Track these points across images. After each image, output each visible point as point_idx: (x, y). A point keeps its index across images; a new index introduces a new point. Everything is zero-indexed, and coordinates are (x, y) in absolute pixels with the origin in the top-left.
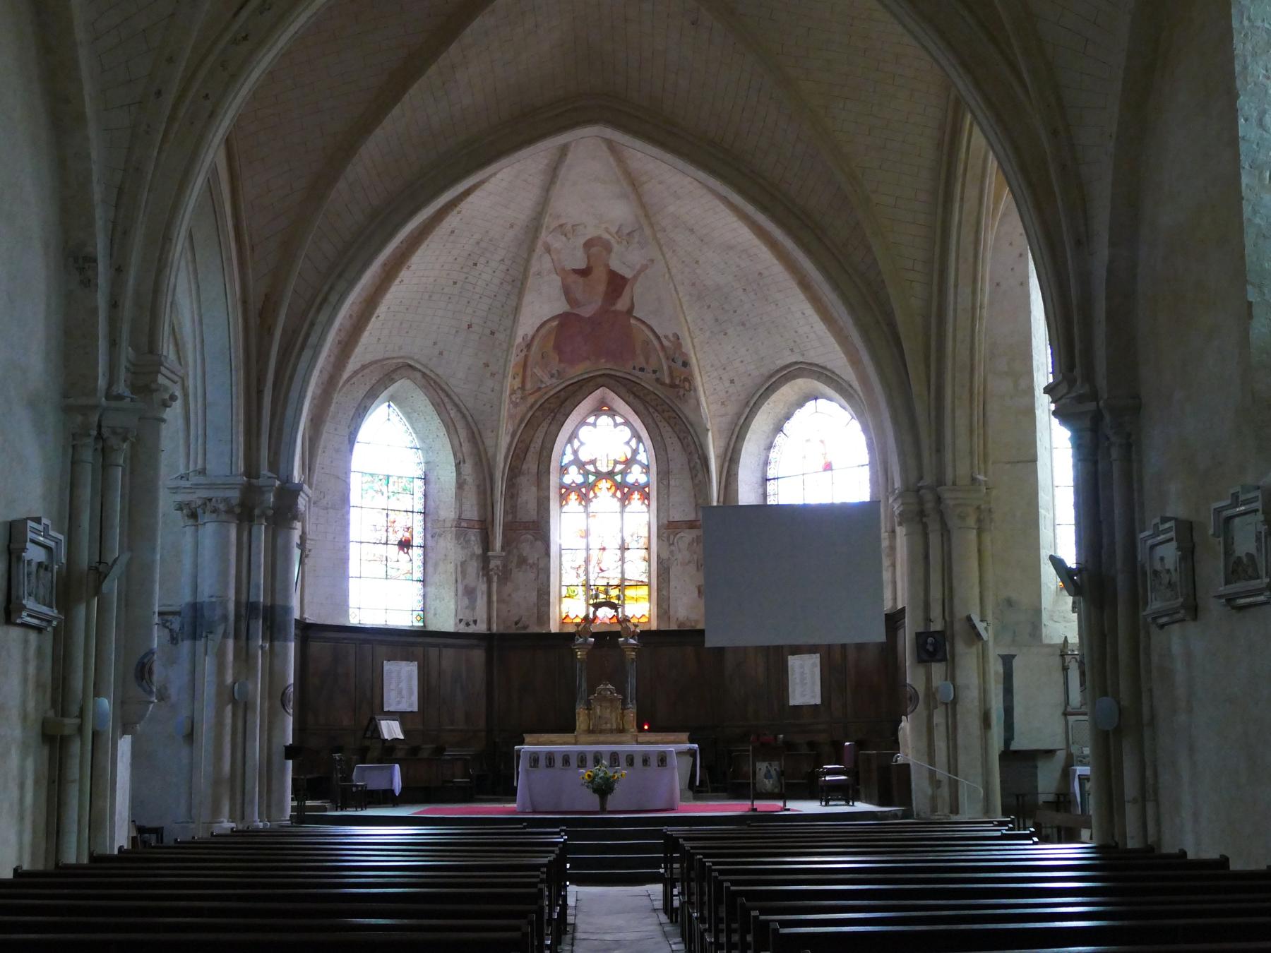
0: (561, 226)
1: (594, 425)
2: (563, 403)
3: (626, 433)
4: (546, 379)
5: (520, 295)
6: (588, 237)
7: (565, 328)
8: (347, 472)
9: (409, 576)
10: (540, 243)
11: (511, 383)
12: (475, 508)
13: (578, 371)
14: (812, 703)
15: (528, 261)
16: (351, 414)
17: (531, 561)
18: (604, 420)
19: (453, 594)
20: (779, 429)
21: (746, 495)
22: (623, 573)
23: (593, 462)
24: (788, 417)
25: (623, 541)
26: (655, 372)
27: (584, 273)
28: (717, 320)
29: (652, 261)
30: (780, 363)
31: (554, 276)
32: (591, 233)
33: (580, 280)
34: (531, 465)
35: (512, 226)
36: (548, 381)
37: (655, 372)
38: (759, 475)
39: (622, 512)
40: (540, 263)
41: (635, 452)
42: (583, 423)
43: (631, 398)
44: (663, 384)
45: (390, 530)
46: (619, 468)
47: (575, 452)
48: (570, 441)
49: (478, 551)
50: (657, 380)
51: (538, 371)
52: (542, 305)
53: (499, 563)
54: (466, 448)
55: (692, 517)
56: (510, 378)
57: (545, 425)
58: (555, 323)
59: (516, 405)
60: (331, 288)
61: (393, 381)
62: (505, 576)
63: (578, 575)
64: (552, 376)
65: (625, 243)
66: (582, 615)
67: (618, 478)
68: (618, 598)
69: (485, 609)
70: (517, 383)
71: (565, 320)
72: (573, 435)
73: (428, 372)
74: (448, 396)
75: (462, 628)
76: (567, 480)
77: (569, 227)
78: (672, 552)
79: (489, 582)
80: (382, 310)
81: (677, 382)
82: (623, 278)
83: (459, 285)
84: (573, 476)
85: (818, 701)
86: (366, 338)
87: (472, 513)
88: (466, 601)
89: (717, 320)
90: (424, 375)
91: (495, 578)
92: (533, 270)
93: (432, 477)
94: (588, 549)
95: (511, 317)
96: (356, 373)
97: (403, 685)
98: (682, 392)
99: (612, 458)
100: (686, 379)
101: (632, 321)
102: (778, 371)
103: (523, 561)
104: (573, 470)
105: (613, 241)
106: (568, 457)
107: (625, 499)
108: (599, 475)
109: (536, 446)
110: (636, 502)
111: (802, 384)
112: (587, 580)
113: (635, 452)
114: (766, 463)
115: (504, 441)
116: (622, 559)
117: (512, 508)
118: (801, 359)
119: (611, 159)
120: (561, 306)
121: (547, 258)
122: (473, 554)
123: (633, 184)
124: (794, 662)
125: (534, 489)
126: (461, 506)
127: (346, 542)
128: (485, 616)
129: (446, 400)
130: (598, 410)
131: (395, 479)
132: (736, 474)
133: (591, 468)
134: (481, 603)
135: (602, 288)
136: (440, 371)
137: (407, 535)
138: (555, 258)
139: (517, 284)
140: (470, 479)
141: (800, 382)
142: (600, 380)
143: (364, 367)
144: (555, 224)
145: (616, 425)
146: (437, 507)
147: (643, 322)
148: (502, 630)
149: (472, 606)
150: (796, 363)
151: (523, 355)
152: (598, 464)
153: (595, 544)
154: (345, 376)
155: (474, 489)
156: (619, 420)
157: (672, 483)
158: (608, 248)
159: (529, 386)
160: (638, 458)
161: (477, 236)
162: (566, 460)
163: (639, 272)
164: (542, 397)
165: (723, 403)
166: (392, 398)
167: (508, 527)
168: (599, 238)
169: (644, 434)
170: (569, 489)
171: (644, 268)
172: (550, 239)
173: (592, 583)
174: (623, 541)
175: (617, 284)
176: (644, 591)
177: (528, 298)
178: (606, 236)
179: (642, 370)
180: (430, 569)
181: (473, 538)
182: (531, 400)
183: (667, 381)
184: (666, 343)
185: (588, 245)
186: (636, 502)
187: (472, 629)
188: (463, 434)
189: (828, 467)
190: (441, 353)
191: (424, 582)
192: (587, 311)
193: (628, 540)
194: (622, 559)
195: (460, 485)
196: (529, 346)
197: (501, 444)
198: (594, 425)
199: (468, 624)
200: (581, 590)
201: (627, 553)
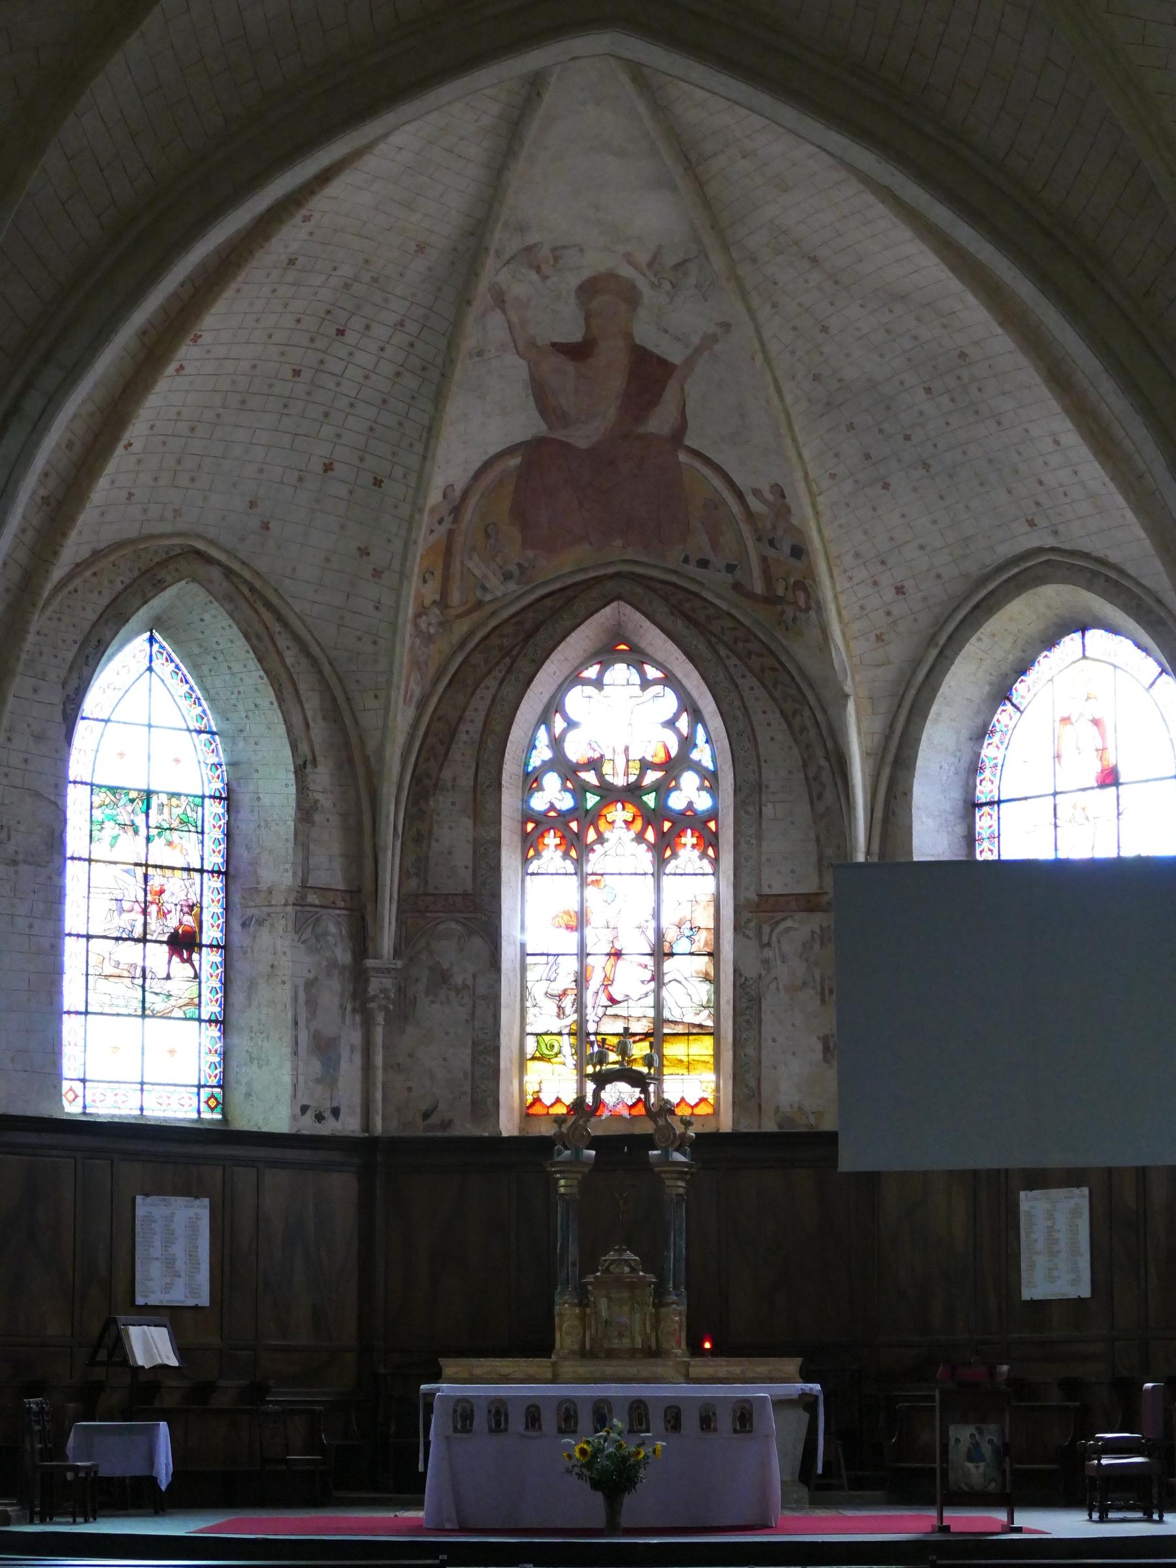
0: (529, 249)
1: (598, 683)
2: (529, 636)
3: (669, 702)
4: (494, 582)
5: (439, 397)
6: (586, 274)
7: (536, 472)
8: (60, 782)
9: (192, 1011)
10: (483, 285)
11: (418, 590)
12: (337, 865)
13: (566, 565)
14: (1071, 1293)
15: (457, 324)
16: (70, 656)
17: (459, 980)
18: (620, 672)
19: (287, 1050)
20: (1002, 694)
21: (930, 840)
22: (658, 1006)
23: (595, 765)
24: (1022, 669)
26: (730, 568)
27: (578, 352)
28: (867, 456)
29: (726, 326)
30: (1006, 550)
31: (511, 358)
32: (595, 262)
33: (570, 367)
34: (460, 769)
35: (421, 249)
36: (498, 587)
37: (730, 568)
38: (956, 794)
39: (658, 875)
40: (486, 329)
41: (687, 743)
42: (574, 679)
43: (680, 625)
44: (751, 596)
45: (153, 909)
46: (652, 777)
47: (556, 743)
48: (545, 719)
49: (343, 956)
50: (737, 587)
51: (477, 567)
52: (487, 421)
53: (388, 983)
54: (319, 731)
55: (809, 885)
56: (415, 580)
57: (492, 683)
58: (514, 462)
59: (429, 639)
60: (28, 386)
61: (160, 586)
62: (402, 1012)
64: (507, 576)
65: (667, 286)
66: (569, 1097)
67: (650, 800)
68: (648, 1061)
69: (357, 1087)
70: (430, 592)
71: (535, 452)
72: (554, 706)
73: (236, 567)
74: (280, 618)
75: (307, 1125)
76: (539, 803)
77: (545, 252)
78: (766, 962)
79: (367, 1025)
80: (137, 431)
81: (780, 592)
82: (662, 362)
83: (306, 375)
84: (552, 794)
85: (1085, 1291)
86: (101, 491)
87: (330, 872)
88: (316, 1067)
89: (867, 456)
90: (228, 572)
91: (380, 1018)
92: (469, 343)
93: (244, 798)
94: (583, 954)
95: (419, 447)
96: (78, 568)
97: (179, 1250)
98: (790, 612)
99: (635, 755)
100: (800, 585)
101: (683, 457)
102: (1000, 569)
103: (441, 978)
104: (552, 781)
105: (642, 284)
106: (542, 754)
107: (663, 848)
108: (609, 794)
109: (471, 729)
110: (688, 855)
111: (1052, 597)
112: (582, 1021)
113: (687, 743)
114: (975, 767)
115: (402, 718)
116: (658, 978)
117: (417, 865)
118: (1050, 542)
119: (641, 107)
120: (525, 424)
121: (496, 320)
122: (333, 963)
123: (688, 161)
124: (1032, 1204)
125: (468, 822)
126: (306, 858)
127: (57, 936)
128: (357, 1099)
129: (277, 628)
130: (605, 655)
131: (163, 798)
132: (908, 794)
133: (590, 777)
134: (350, 1068)
135: (617, 382)
136: (262, 565)
137: (189, 920)
138: (515, 319)
139: (432, 375)
140: (326, 801)
141: (1049, 592)
142: (610, 585)
143: (97, 555)
144: (514, 245)
145: (645, 684)
146: (254, 863)
147: (708, 461)
148: (395, 1130)
149: (329, 1078)
150: (1040, 550)
151: (443, 528)
152: (607, 769)
153: (598, 942)
154: (57, 573)
155: (335, 820)
156: (652, 672)
157: (768, 810)
158: (631, 297)
159: (455, 597)
160: (695, 755)
161: (346, 271)
162: (535, 761)
163: (698, 351)
164: (484, 623)
165: (879, 638)
166: (158, 624)
167: (410, 906)
168: (611, 276)
169: (708, 705)
170: (544, 822)
171: (710, 340)
172: (503, 278)
173: (591, 1028)
175: (649, 375)
176: (704, 1047)
177: (455, 406)
178: (626, 271)
179: (703, 563)
180: (238, 998)
181: (332, 929)
182: (461, 628)
183: (759, 588)
184: (755, 505)
185: (589, 289)
186: (688, 855)
187: (330, 1127)
188: (312, 702)
189: (1110, 778)
190: (266, 526)
191: (223, 1023)
192: (583, 437)
193: (670, 934)
194: (658, 978)
195: (306, 811)
196: (456, 512)
197: (397, 725)
198: (598, 683)
199: (319, 1117)
200: (566, 1042)
201: (669, 965)
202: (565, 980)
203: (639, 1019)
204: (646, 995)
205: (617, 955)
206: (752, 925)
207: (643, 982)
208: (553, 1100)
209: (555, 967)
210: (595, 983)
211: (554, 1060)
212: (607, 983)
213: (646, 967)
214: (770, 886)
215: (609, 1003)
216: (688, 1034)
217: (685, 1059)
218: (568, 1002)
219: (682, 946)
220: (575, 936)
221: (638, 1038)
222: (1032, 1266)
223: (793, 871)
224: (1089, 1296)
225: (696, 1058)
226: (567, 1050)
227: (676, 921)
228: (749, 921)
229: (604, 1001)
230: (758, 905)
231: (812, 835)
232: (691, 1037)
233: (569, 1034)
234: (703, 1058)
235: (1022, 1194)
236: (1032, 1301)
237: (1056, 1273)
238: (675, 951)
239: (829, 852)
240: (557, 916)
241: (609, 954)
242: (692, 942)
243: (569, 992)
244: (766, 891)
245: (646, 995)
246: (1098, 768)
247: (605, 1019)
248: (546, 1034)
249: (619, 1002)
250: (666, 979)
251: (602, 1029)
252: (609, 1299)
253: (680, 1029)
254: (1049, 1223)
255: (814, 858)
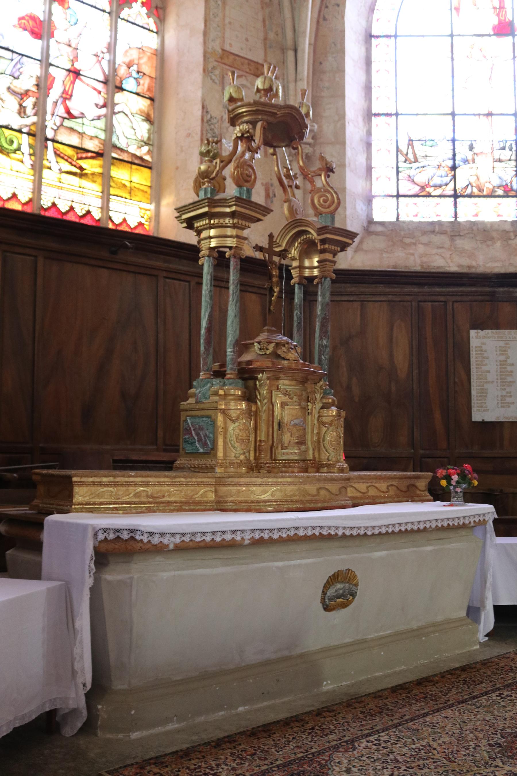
25: (112, 63)
39: (114, 14)
63: (22, 111)
66: (25, 196)
94: (46, 62)
110: (137, 11)
116: (108, 104)
153: (60, 57)
174: (112, 63)
193: (122, 71)
194: (108, 104)
201: (119, 97)
202: (27, 83)
203: (91, 138)
204: (99, 118)
205: (76, 73)
206: (217, 72)
207: (97, 105)
208: (10, 195)
209: (19, 66)
210: (55, 93)
211: (12, 155)
212: (66, 96)
213: (100, 92)
214: (231, 45)
215: (66, 115)
216: (132, 163)
217: (128, 184)
218: (29, 103)
219: (129, 84)
220: (39, 43)
221: (90, 154)
222: (483, 393)
223: (247, 40)
224: (474, 420)
225: (137, 186)
226: (25, 149)
227: (127, 60)
228: (214, 68)
229: (61, 110)
230: (222, 58)
231: (260, 17)
232: (134, 167)
233: (29, 134)
234: (142, 188)
235: (473, 333)
236: (484, 423)
237: (508, 400)
238: (124, 86)
239: (271, 35)
240: (23, 18)
241: (69, 71)
242: (139, 84)
243: (30, 93)
244: (227, 48)
245: (99, 118)
246: (495, 21)
247: (62, 130)
248: (7, 127)
249: (75, 117)
250: (117, 109)
251: (59, 138)
252: (286, 393)
253: (125, 157)
254: (502, 358)
255: (261, 35)
